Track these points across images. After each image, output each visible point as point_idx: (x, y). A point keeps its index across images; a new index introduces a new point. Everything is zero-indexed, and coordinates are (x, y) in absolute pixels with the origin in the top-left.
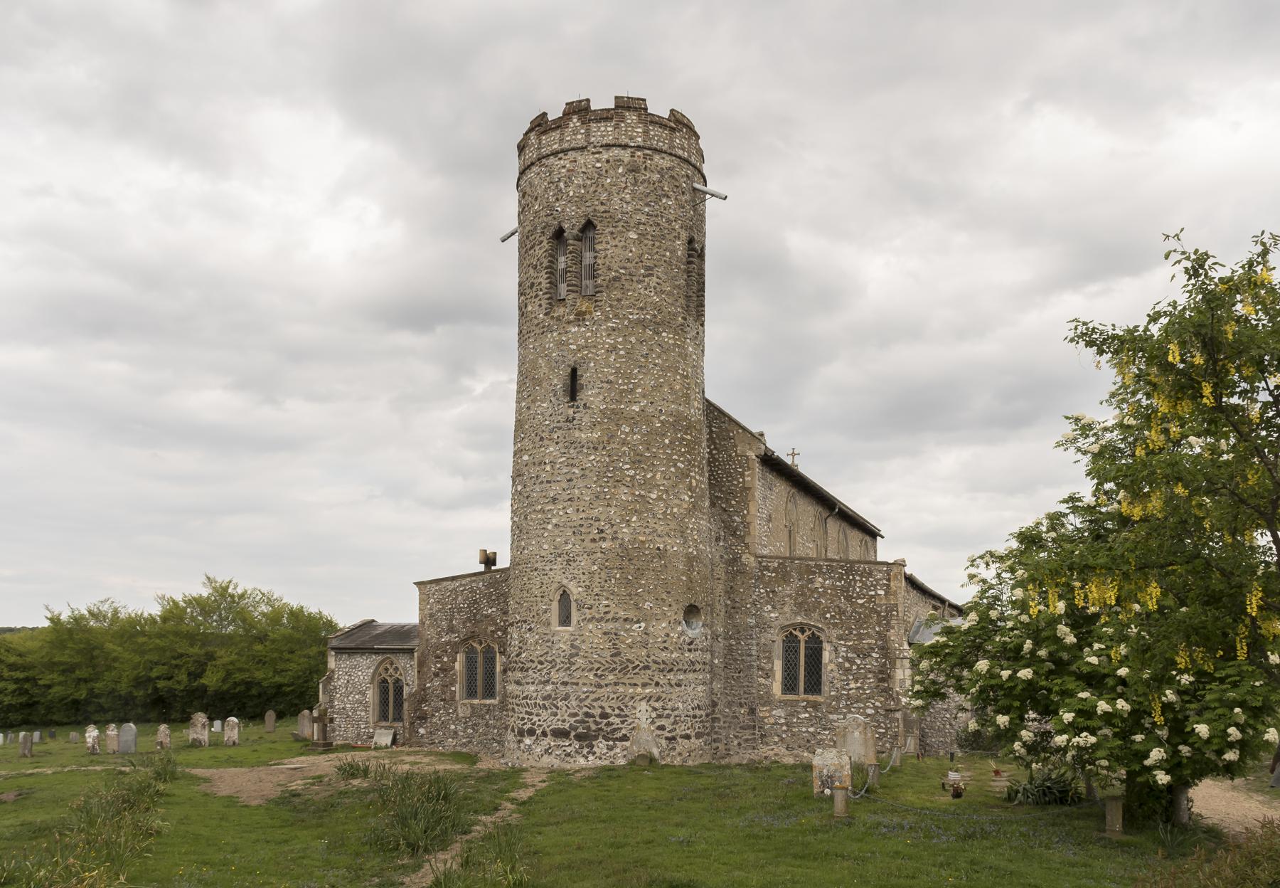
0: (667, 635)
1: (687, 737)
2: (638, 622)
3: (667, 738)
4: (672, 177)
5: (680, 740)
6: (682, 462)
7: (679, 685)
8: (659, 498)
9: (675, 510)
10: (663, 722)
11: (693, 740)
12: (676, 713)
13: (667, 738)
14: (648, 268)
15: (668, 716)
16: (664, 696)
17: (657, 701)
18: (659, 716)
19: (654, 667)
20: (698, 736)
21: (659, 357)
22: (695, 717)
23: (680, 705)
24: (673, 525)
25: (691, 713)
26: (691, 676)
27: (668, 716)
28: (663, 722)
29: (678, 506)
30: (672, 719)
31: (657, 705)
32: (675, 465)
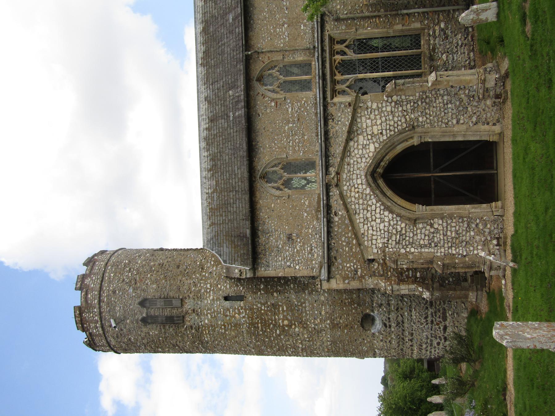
0: (382, 341)
1: (445, 328)
2: (375, 352)
3: (445, 341)
4: (117, 337)
5: (447, 333)
6: (276, 331)
7: (412, 334)
8: (301, 343)
9: (306, 337)
10: (435, 343)
11: (447, 323)
12: (429, 337)
13: (445, 341)
14: (174, 345)
15: (431, 341)
16: (419, 343)
17: (422, 346)
18: (431, 345)
19: (401, 347)
20: (445, 319)
21: (220, 342)
22: (432, 322)
23: (424, 334)
24: (315, 337)
25: (430, 325)
26: (406, 325)
27: (431, 341)
28: (435, 343)
29: (303, 335)
30: (433, 339)
31: (424, 346)
32: (279, 335)
